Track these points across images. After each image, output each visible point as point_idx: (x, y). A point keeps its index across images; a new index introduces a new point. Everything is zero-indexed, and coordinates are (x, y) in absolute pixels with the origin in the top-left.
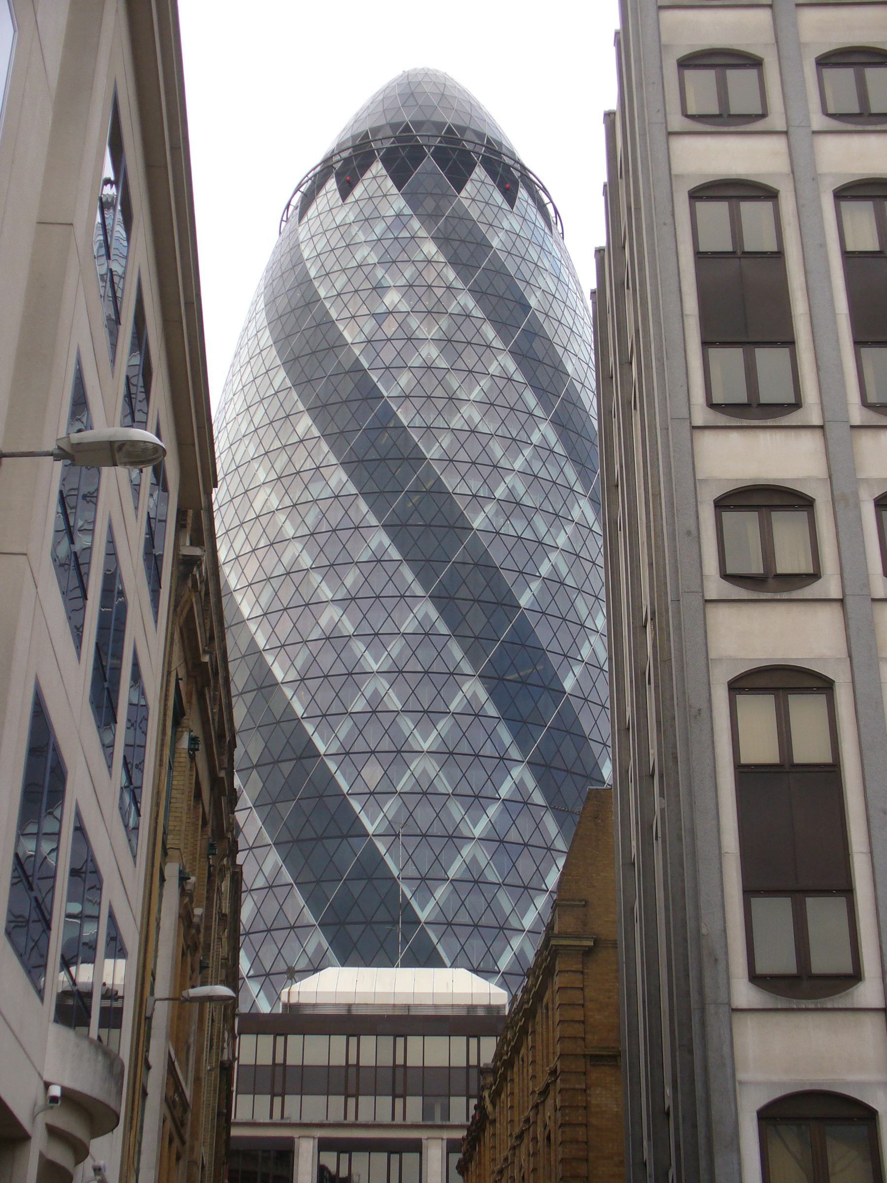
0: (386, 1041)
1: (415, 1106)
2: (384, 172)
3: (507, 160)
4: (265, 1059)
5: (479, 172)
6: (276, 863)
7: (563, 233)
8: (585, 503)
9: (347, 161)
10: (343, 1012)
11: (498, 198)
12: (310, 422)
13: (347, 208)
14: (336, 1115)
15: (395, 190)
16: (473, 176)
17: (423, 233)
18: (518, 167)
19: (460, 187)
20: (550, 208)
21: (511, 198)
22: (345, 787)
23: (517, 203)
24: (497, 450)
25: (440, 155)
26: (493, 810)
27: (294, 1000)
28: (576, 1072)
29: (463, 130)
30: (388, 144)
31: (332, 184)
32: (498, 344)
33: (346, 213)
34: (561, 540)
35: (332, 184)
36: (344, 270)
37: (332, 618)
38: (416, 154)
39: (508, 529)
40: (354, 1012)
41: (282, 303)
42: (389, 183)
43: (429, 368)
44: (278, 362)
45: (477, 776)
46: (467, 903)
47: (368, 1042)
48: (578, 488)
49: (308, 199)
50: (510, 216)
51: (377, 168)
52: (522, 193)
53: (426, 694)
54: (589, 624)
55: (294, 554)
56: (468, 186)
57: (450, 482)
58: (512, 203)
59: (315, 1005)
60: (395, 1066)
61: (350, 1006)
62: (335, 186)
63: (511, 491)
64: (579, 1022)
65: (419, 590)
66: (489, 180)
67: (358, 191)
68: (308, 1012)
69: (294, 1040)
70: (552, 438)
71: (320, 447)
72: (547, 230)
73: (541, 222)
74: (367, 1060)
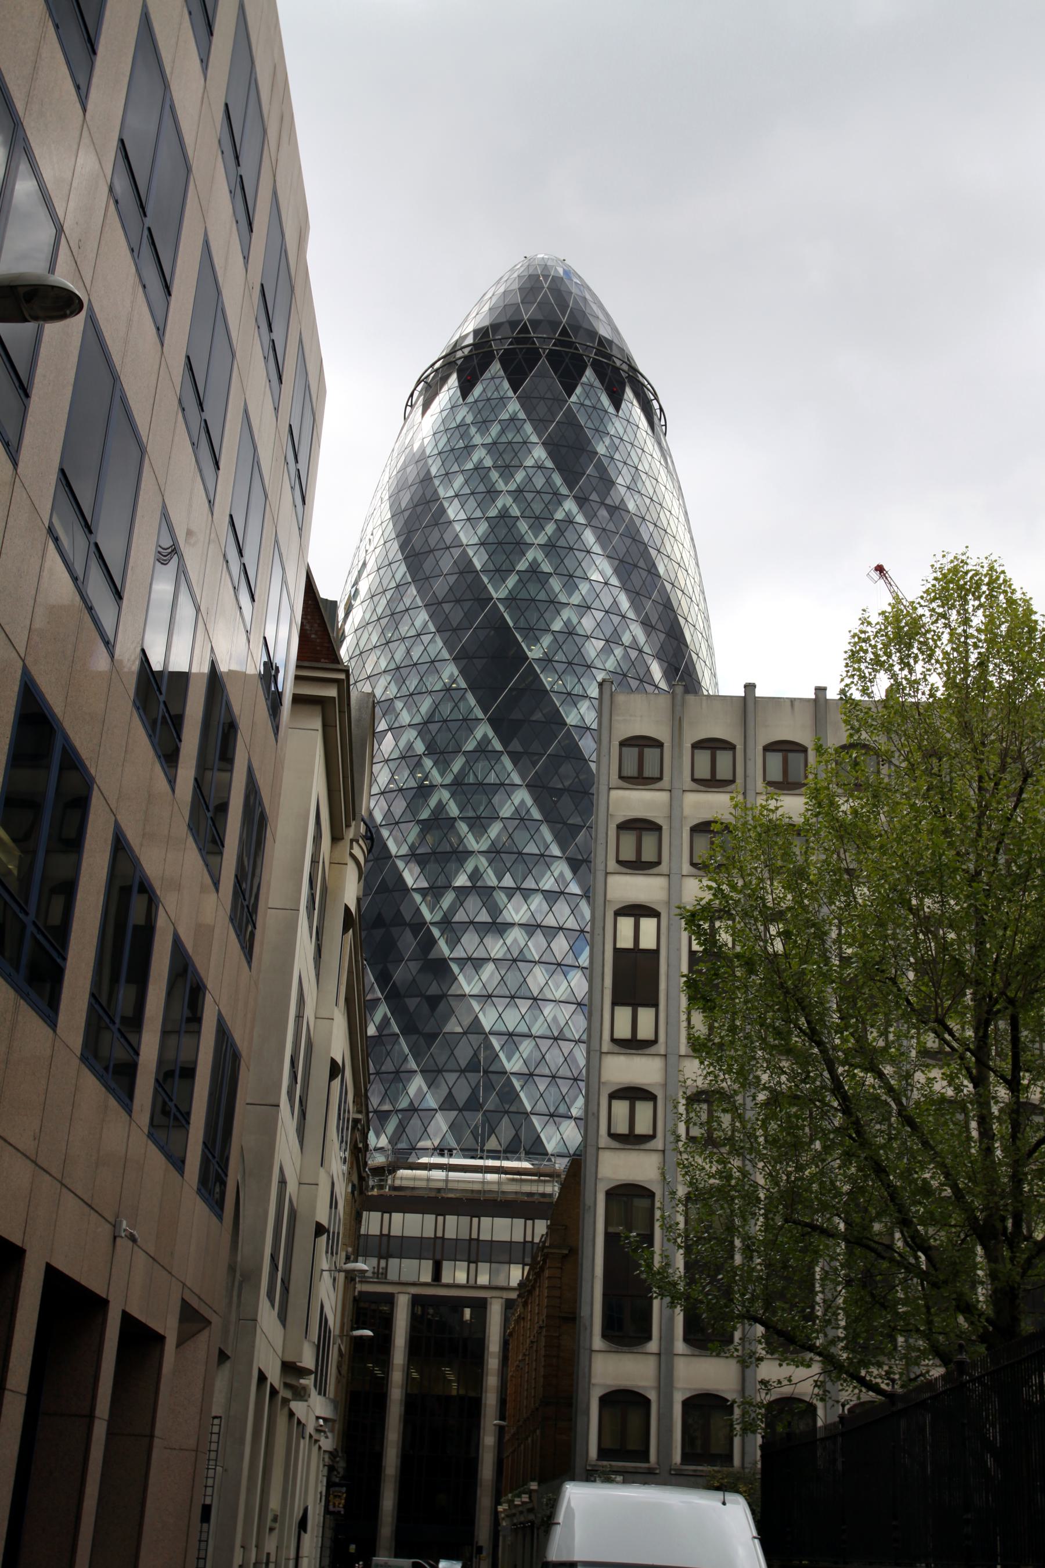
2: (502, 373)
5: (589, 374)
9: (466, 358)
11: (605, 400)
15: (510, 393)
16: (584, 379)
17: (534, 438)
19: (570, 392)
25: (554, 358)
31: (453, 380)
38: (533, 356)
41: (405, 499)
42: (506, 385)
44: (400, 556)
51: (496, 367)
55: (409, 739)
56: (578, 390)
62: (456, 384)
66: (597, 383)
67: (477, 391)
71: (435, 642)
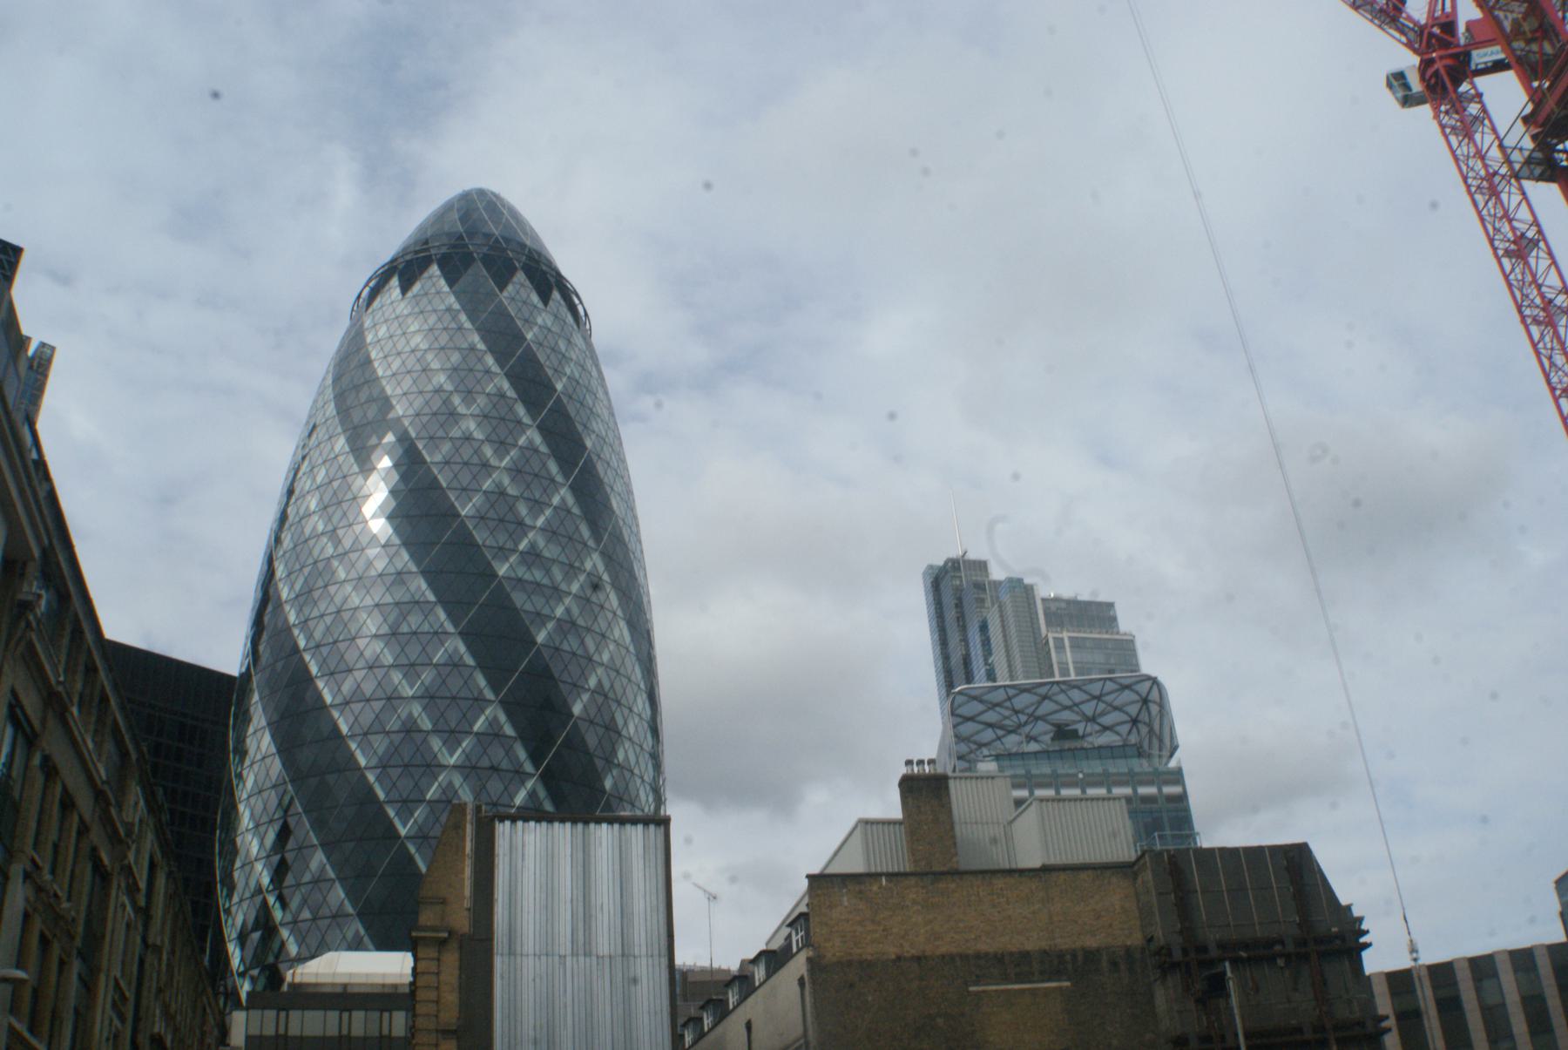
0: (375, 1015)
2: (438, 273)
3: (544, 268)
4: (269, 1031)
5: (520, 276)
6: (321, 861)
7: (590, 330)
8: (596, 556)
10: (339, 990)
11: (535, 298)
13: (406, 302)
15: (446, 289)
18: (554, 274)
19: (502, 288)
20: (580, 308)
21: (545, 298)
22: (381, 795)
23: (551, 303)
24: (523, 509)
27: (297, 980)
28: (429, 1044)
29: (507, 240)
30: (444, 250)
31: (395, 282)
32: (527, 420)
33: (403, 308)
34: (575, 588)
35: (395, 282)
36: (399, 354)
37: (375, 651)
38: (468, 260)
39: (527, 577)
40: (350, 990)
42: (443, 282)
43: (468, 438)
47: (358, 1015)
49: (375, 292)
50: (544, 314)
51: (434, 269)
52: (556, 295)
53: (453, 717)
54: (596, 658)
56: (510, 288)
57: (480, 537)
60: (381, 1037)
61: (345, 986)
64: (433, 1002)
65: (450, 628)
67: (416, 288)
68: (311, 990)
69: (295, 1015)
70: (570, 500)
72: (575, 327)
73: (570, 319)
74: (358, 1030)
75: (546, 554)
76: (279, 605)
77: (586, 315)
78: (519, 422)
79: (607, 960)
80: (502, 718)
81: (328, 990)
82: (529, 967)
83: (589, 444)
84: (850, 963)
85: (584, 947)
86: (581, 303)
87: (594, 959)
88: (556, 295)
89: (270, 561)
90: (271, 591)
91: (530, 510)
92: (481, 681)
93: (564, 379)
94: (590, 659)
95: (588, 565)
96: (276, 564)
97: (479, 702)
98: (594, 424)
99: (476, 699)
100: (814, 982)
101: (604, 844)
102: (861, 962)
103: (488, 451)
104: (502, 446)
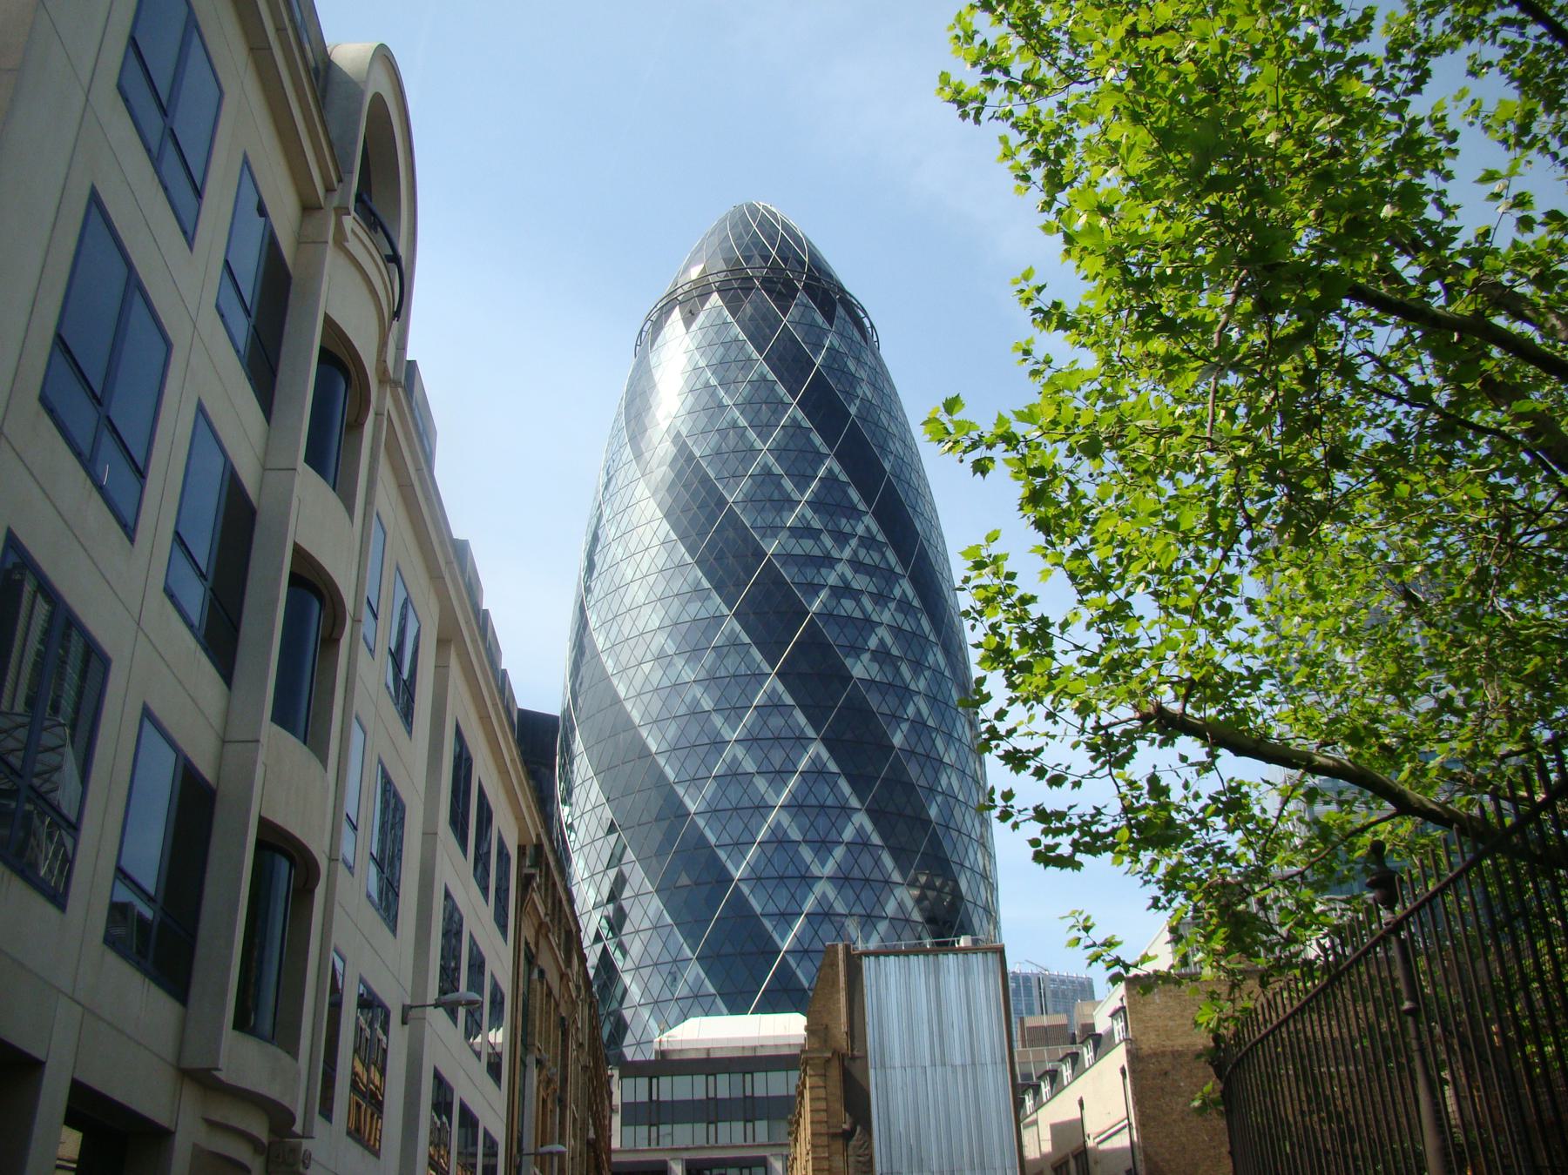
0: (737, 1077)
1: (761, 1126)
2: (720, 302)
4: (643, 1097)
6: (658, 907)
10: (703, 1055)
11: (820, 319)
12: (668, 527)
14: (701, 1141)
21: (830, 318)
22: (712, 839)
26: (839, 852)
27: (665, 1047)
32: (824, 449)
35: (676, 314)
37: (694, 696)
40: (713, 1055)
45: (822, 823)
46: (820, 933)
47: (723, 1079)
48: (898, 570)
51: (715, 299)
52: (840, 311)
53: (777, 758)
58: (830, 321)
59: (681, 1051)
60: (745, 1097)
61: (708, 1050)
63: (842, 577)
68: (675, 1057)
69: (665, 1081)
72: (863, 343)
74: (723, 1093)
75: (855, 585)
76: (596, 655)
77: (872, 326)
78: (818, 452)
79: (960, 1070)
80: (825, 755)
81: (693, 1055)
82: (897, 1077)
83: (887, 466)
84: (1164, 1054)
85: (941, 1059)
86: (866, 315)
87: (949, 1069)
88: (840, 311)
89: (582, 610)
90: (586, 641)
91: (835, 540)
92: (801, 719)
93: (858, 402)
94: (907, 688)
95: (897, 592)
96: (588, 613)
97: (801, 741)
98: (891, 444)
99: (798, 738)
100: (1133, 1071)
101: (952, 970)
102: (1173, 1053)
103: (788, 484)
104: (802, 481)
